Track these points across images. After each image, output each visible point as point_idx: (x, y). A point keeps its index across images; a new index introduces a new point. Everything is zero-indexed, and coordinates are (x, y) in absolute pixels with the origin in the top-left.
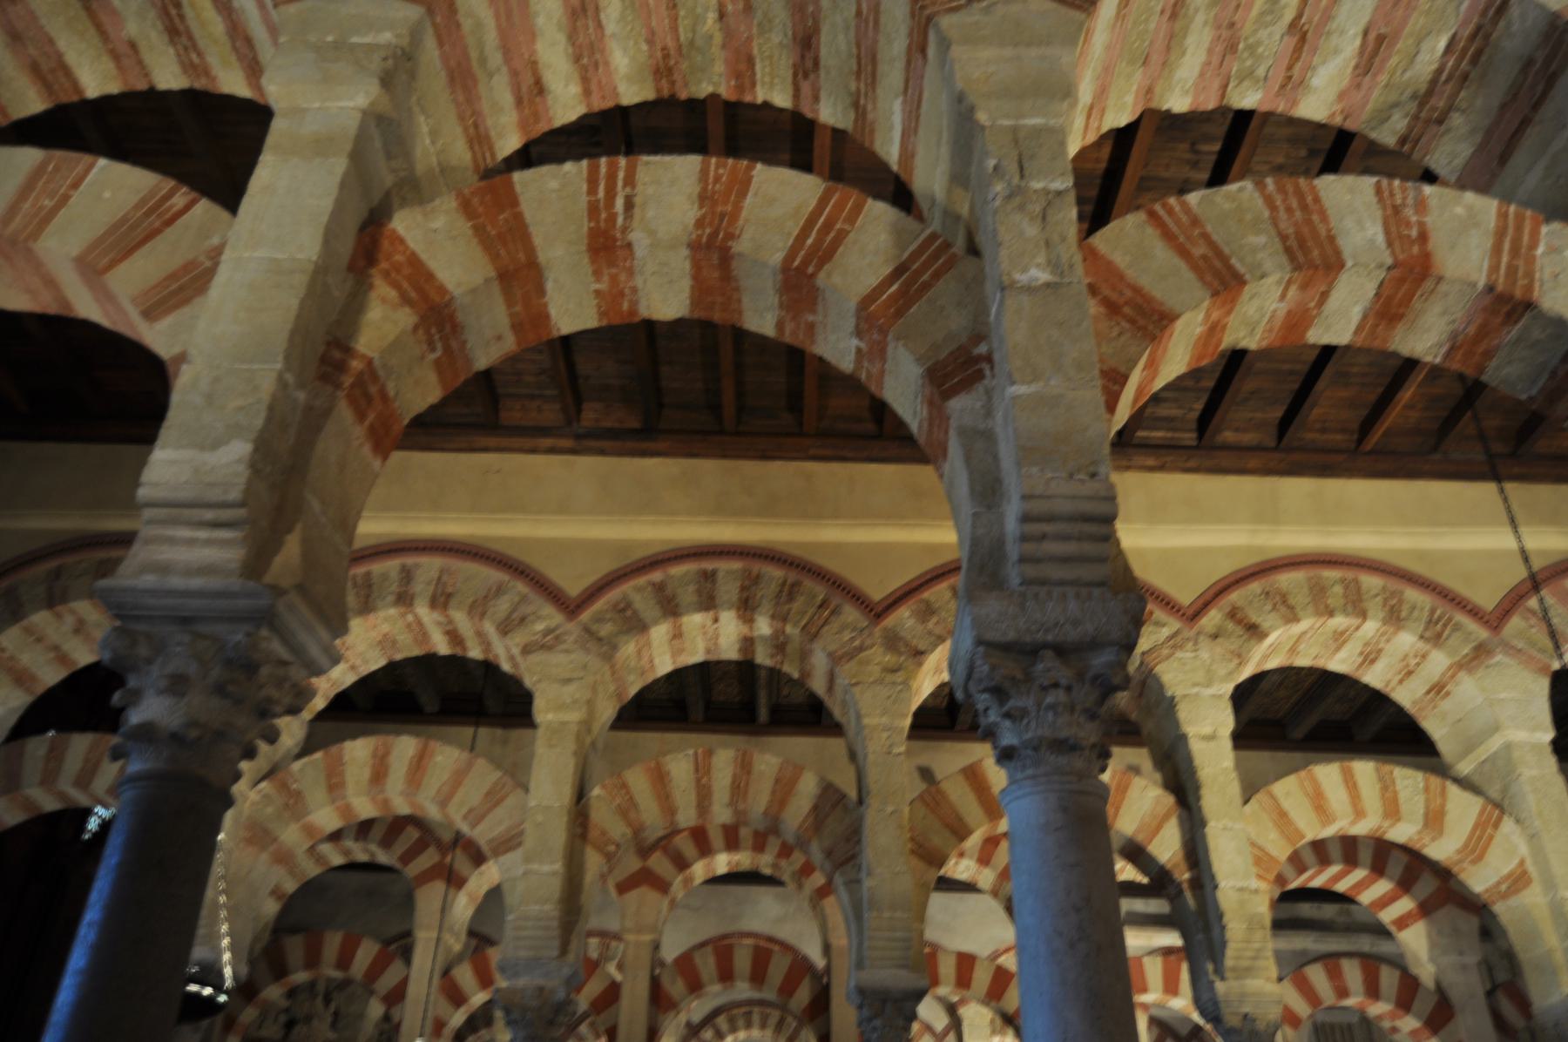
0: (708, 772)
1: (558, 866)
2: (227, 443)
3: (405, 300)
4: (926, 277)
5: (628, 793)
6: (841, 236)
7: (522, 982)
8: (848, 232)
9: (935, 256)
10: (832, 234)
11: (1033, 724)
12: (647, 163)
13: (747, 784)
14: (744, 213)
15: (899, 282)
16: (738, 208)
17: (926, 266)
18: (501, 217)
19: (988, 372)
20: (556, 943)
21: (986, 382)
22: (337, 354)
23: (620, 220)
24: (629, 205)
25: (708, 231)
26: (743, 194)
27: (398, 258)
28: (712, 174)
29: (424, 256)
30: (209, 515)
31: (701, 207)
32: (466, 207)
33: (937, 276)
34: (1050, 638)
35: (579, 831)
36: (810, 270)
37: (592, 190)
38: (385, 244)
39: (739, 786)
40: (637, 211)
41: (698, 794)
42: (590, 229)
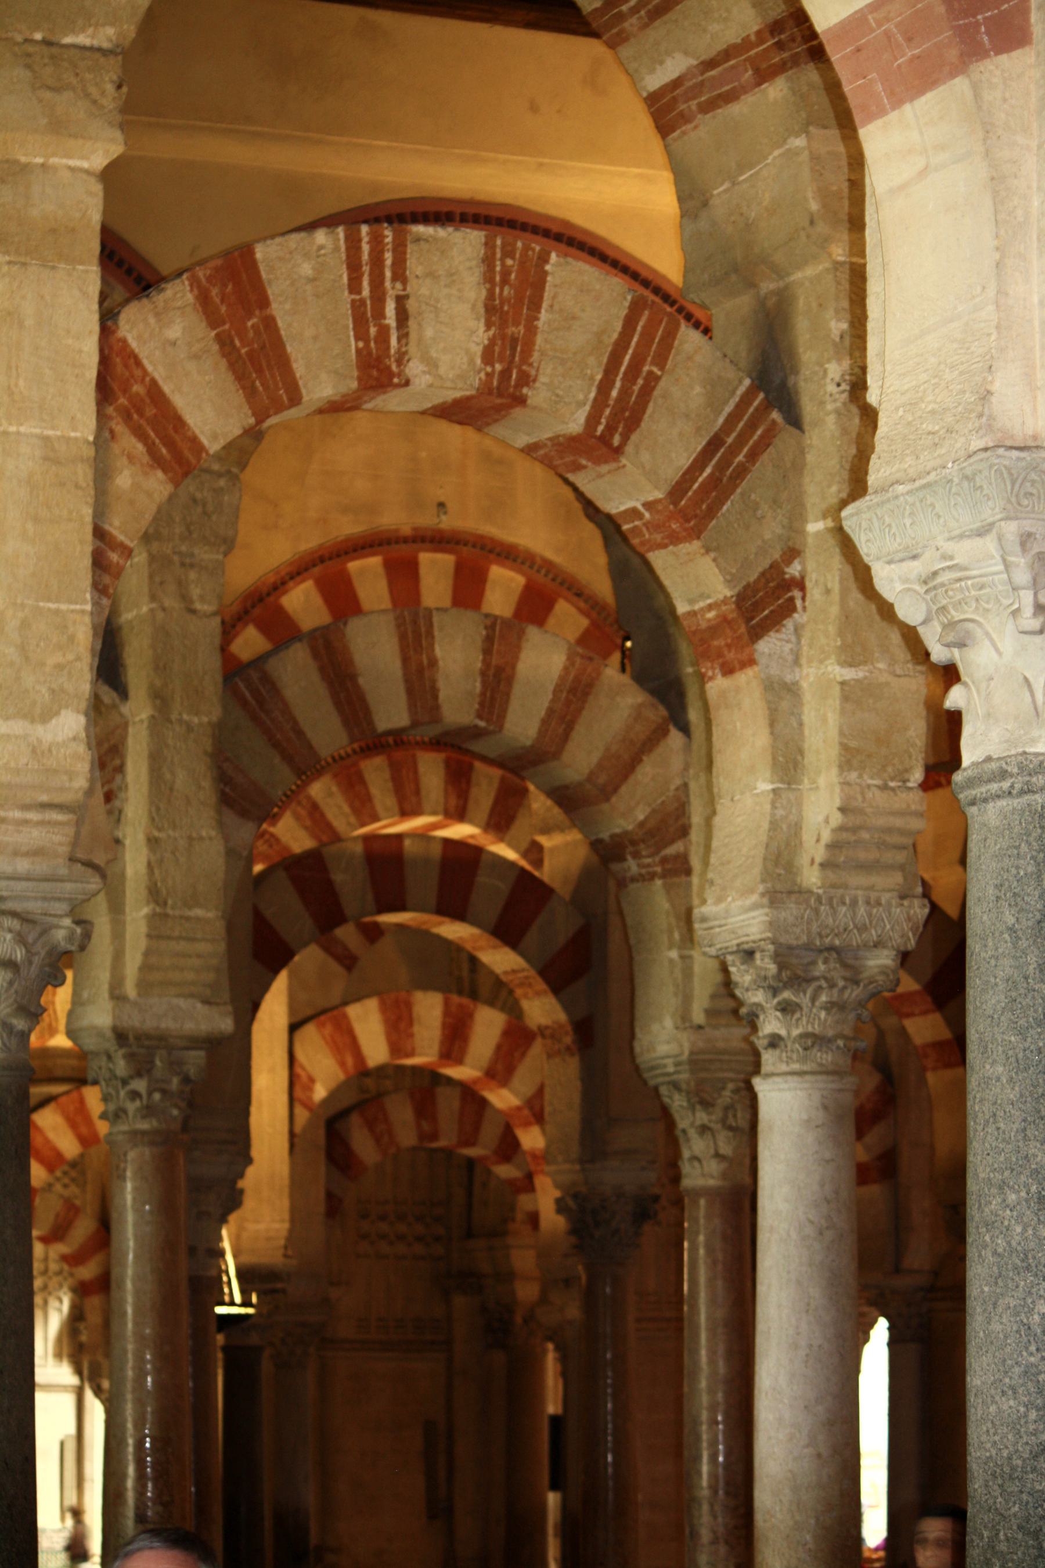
2: (57, 713)
3: (157, 461)
4: (741, 458)
6: (652, 380)
9: (752, 426)
10: (640, 382)
11: (804, 1019)
12: (418, 240)
14: (539, 340)
16: (531, 330)
17: (741, 440)
18: (250, 324)
19: (799, 603)
21: (796, 615)
23: (394, 341)
25: (498, 367)
26: (536, 305)
27: (137, 388)
29: (167, 388)
30: (44, 798)
31: (488, 326)
32: (204, 300)
33: (753, 456)
34: (837, 942)
36: (616, 440)
37: (354, 286)
40: (412, 324)
42: (358, 351)
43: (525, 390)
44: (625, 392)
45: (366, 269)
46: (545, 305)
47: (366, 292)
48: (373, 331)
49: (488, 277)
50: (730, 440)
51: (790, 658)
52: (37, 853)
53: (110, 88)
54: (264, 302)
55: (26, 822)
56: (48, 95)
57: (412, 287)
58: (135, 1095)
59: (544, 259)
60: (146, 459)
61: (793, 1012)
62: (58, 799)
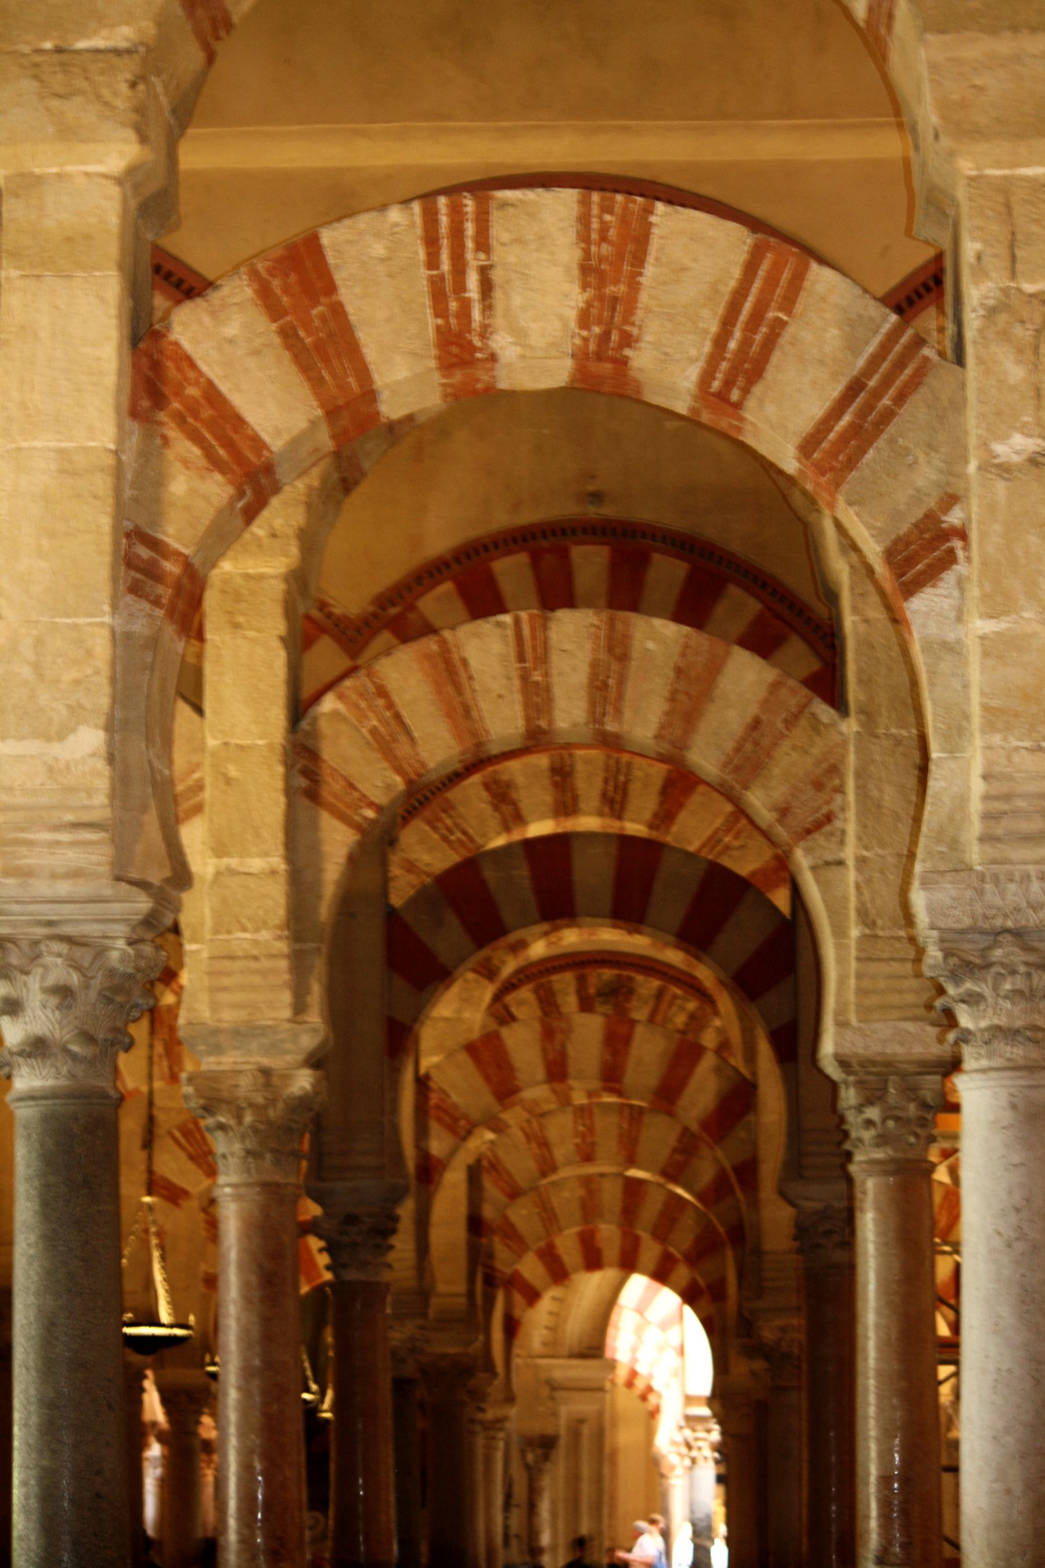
0: (543, 658)
1: (278, 862)
2: (73, 730)
3: (215, 463)
4: (886, 401)
5: (390, 706)
6: (778, 326)
7: (227, 1061)
8: (786, 323)
9: (900, 365)
10: (764, 329)
12: (504, 205)
13: (621, 682)
14: (644, 298)
15: (851, 410)
16: (634, 287)
17: (887, 381)
18: (314, 312)
19: (960, 554)
20: (286, 997)
22: (144, 552)
23: (476, 315)
24: (487, 287)
25: (597, 330)
26: (639, 260)
27: (192, 391)
28: (595, 225)
29: (224, 387)
30: (70, 817)
31: (585, 286)
32: (265, 294)
33: (901, 398)
34: (1009, 924)
35: (302, 782)
36: (735, 395)
37: (433, 262)
38: (171, 371)
39: (605, 686)
40: (498, 294)
41: (527, 704)
42: (438, 328)
43: (627, 352)
44: (746, 343)
45: (445, 243)
46: (650, 259)
47: (446, 266)
48: (453, 305)
49: (584, 237)
50: (872, 383)
51: (952, 615)
52: (75, 874)
53: (124, 88)
54: (331, 288)
55: (58, 843)
56: (55, 103)
57: (499, 254)
58: (869, 1123)
59: (649, 211)
60: (203, 462)
61: (977, 1003)
62: (86, 818)
